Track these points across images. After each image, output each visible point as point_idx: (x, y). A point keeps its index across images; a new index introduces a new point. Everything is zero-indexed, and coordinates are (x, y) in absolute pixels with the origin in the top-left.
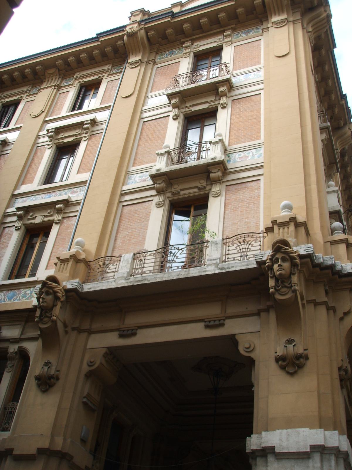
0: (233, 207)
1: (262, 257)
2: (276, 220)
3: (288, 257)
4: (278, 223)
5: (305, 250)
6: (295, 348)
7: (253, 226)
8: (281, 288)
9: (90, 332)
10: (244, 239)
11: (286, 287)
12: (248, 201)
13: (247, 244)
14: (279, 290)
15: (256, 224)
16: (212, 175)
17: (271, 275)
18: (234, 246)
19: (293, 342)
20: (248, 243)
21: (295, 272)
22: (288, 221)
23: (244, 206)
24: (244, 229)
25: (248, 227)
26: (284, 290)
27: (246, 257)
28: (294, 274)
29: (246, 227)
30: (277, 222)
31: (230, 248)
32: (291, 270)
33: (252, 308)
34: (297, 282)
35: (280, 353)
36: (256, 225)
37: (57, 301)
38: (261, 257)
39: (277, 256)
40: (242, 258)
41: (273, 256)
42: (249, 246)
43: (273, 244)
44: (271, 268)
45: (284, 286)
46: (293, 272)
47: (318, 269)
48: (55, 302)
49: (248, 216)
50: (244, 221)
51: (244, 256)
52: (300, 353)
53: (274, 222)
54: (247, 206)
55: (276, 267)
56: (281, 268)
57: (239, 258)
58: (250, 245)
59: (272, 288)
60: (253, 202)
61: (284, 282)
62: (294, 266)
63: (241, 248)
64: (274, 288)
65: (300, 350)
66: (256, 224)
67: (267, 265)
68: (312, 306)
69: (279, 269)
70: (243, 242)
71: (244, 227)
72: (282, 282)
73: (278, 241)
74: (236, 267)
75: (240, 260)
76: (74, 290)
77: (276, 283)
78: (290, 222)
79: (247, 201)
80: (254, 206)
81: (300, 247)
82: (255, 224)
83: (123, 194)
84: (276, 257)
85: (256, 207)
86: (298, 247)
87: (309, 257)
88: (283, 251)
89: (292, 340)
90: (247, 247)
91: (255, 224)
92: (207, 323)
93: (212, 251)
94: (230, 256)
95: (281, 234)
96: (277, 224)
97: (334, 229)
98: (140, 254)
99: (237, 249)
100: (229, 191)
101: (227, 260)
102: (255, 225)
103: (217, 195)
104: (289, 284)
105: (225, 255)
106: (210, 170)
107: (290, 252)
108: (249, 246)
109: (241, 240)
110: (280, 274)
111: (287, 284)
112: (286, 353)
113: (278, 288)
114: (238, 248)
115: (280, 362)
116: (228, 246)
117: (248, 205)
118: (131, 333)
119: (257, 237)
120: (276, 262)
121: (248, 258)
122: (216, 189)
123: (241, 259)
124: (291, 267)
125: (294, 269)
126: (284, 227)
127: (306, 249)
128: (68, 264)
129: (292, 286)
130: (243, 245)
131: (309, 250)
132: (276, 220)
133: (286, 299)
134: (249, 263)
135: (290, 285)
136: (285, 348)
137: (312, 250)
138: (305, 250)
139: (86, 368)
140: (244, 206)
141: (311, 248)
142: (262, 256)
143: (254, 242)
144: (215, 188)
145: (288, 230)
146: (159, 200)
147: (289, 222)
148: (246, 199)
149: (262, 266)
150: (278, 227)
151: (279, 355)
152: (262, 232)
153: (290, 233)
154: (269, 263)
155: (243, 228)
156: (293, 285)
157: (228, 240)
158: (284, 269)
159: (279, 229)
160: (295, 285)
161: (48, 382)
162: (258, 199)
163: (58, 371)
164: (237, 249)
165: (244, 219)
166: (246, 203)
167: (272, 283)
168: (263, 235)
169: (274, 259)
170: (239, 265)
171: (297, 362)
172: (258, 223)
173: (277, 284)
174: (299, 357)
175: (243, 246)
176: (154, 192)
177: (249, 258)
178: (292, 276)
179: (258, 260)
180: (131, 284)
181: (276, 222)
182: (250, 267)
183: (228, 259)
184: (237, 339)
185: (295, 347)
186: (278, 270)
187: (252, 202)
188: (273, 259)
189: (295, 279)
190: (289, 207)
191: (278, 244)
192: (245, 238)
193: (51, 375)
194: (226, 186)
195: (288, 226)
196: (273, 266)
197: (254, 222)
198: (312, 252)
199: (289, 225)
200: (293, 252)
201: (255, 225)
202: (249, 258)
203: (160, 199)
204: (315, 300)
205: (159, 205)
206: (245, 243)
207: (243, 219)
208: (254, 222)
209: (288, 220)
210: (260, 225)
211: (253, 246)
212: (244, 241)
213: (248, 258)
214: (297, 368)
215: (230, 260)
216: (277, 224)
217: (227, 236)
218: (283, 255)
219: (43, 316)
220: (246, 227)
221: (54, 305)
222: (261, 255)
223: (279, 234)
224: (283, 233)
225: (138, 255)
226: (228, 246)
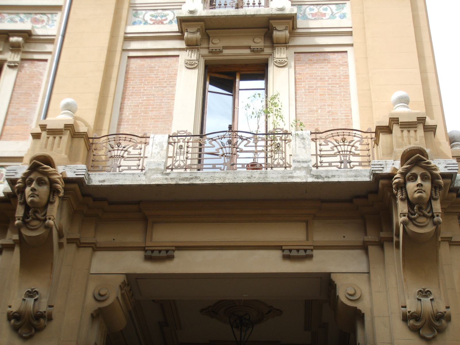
0: (309, 87)
1: (383, 168)
2: (398, 118)
3: (429, 175)
5: (446, 167)
6: (434, 304)
7: (342, 119)
8: (417, 217)
9: (96, 248)
10: (342, 137)
11: (424, 216)
12: (330, 80)
13: (348, 145)
14: (415, 219)
15: (346, 116)
16: (276, 34)
17: (402, 196)
18: (328, 145)
19: (428, 294)
20: (350, 144)
21: (437, 197)
22: (416, 122)
23: (324, 87)
24: (328, 121)
25: (333, 119)
27: (348, 164)
28: (435, 199)
29: (331, 118)
31: (324, 148)
32: (431, 194)
33: (353, 236)
36: (346, 118)
37: (53, 195)
38: (382, 169)
39: (414, 171)
40: (343, 164)
41: (408, 170)
42: (351, 149)
43: (405, 151)
44: (402, 186)
45: (422, 214)
46: (435, 197)
47: (454, 195)
48: (51, 197)
49: (332, 103)
50: (327, 110)
51: (345, 162)
53: (394, 120)
54: (330, 88)
55: (411, 186)
57: (339, 164)
58: (354, 148)
59: (404, 216)
60: (339, 84)
62: (435, 188)
63: (340, 150)
64: (407, 215)
66: (346, 116)
67: (396, 181)
68: (447, 244)
69: (418, 190)
70: (342, 141)
71: (327, 117)
72: (420, 209)
73: (412, 150)
74: (339, 176)
75: (340, 168)
76: (79, 182)
77: (411, 211)
78: (418, 123)
79: (329, 81)
80: (340, 89)
81: (438, 162)
82: (345, 116)
83: (127, 39)
84: (411, 173)
85: (344, 92)
86: (435, 162)
88: (424, 165)
89: (428, 291)
90: (349, 150)
91: (345, 116)
92: (287, 253)
93: (297, 148)
94: (324, 159)
95: (406, 139)
97: (453, 139)
98: (179, 138)
99: (333, 150)
100: (299, 62)
101: (319, 164)
102: (344, 117)
103: (282, 65)
105: (316, 155)
106: (272, 26)
107: (433, 168)
108: (351, 149)
109: (339, 138)
111: (426, 213)
112: (420, 309)
113: (413, 217)
114: (335, 148)
116: (320, 145)
117: (332, 87)
118: (167, 255)
119: (362, 137)
120: (412, 179)
121: (352, 166)
122: (280, 54)
123: (341, 166)
124: (432, 190)
125: (435, 191)
126: (409, 129)
127: (447, 165)
128: (61, 138)
129: (433, 217)
130: (343, 146)
131: (453, 168)
132: (398, 118)
133: (424, 233)
134: (358, 173)
135: (430, 214)
136: (419, 302)
137: (457, 168)
138: (446, 167)
139: (92, 305)
140: (324, 87)
141: (455, 165)
142: (382, 166)
143: (359, 143)
144: (279, 54)
145: (416, 135)
146: (191, 57)
147: (417, 123)
148: (327, 78)
149: (382, 182)
150: (400, 128)
151: (411, 311)
152: (369, 131)
153: (418, 139)
154: (400, 179)
155: (326, 119)
156: (435, 214)
157: (318, 135)
158: (424, 191)
159: (402, 131)
160: (438, 216)
161: (35, 323)
162: (346, 80)
163: (50, 306)
164: (333, 150)
165: (327, 107)
166: (328, 84)
167: (402, 207)
168: (371, 135)
169: (409, 174)
170: (343, 174)
171: (437, 324)
172: (348, 116)
175: (342, 147)
176: (181, 44)
177: (354, 166)
179: (377, 172)
180: (174, 182)
182: (359, 179)
183: (321, 162)
184: (333, 280)
185: (432, 302)
186: (416, 191)
187: (337, 84)
188: (408, 176)
189: (437, 206)
190: (404, 101)
191: (418, 155)
192: (345, 137)
193: (40, 312)
194: (295, 53)
195: (415, 129)
196: (405, 183)
197: (342, 114)
198: (456, 171)
199: (416, 127)
200: (436, 168)
201: (344, 117)
202: (353, 165)
203: (193, 56)
204: (451, 238)
205: (190, 66)
206: (345, 143)
207: (325, 105)
208: (342, 114)
209: (416, 121)
210: (352, 118)
211: (357, 149)
212: (344, 140)
213: (352, 166)
214: (436, 332)
215: (324, 164)
216: (399, 123)
217: (317, 129)
218: (422, 171)
219: (30, 218)
220: (331, 118)
221: (49, 202)
222: (381, 165)
224: (409, 137)
225: (175, 138)
226: (320, 145)
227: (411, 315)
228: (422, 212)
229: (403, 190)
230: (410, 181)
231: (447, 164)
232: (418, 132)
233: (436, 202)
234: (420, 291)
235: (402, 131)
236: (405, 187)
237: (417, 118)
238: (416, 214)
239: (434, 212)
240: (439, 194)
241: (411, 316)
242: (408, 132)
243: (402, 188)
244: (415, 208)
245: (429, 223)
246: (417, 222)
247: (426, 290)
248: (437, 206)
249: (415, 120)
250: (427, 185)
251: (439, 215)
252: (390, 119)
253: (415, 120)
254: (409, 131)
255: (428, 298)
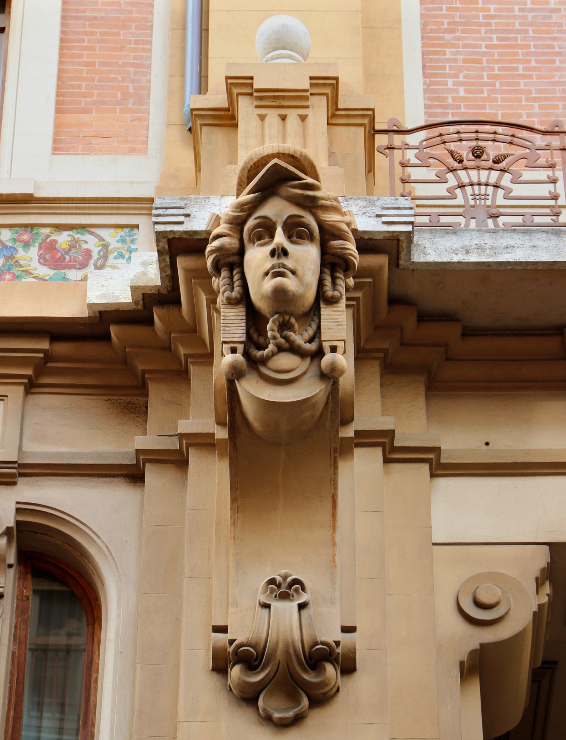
4: (258, 91)
8: (273, 354)
21: (336, 293)
22: (306, 91)
26: (286, 361)
28: (332, 301)
30: (256, 86)
34: (345, 338)
35: (240, 633)
52: (324, 639)
55: (257, 258)
56: (284, 266)
61: (290, 327)
65: (330, 634)
69: (273, 267)
87: (391, 246)
89: (296, 581)
96: (255, 94)
104: (310, 341)
110: (280, 293)
113: (259, 354)
115: (236, 672)
124: (322, 272)
129: (319, 353)
135: (313, 347)
138: (378, 216)
158: (294, 273)
159: (262, 118)
160: (334, 349)
173: (255, 336)
174: (319, 656)
178: (322, 310)
181: (252, 85)
185: (304, 612)
186: (267, 274)
195: (303, 112)
196: (241, 252)
199: (307, 107)
204: (391, 434)
209: (307, 86)
216: (255, 94)
223: (260, 137)
227: (236, 652)
228: (287, 339)
229: (235, 272)
230: (254, 243)
231: (384, 208)
232: (311, 119)
233: (335, 309)
234: (272, 581)
235: (262, 118)
236: (241, 264)
237: (311, 78)
238: (271, 347)
239: (323, 338)
240: (346, 282)
241: (236, 654)
242: (280, 120)
243: (231, 268)
244: (269, 326)
245: (304, 373)
246: (270, 369)
247: (289, 579)
248: (337, 324)
249: (305, 84)
250: (306, 257)
251: (338, 349)
252: (229, 81)
253: (305, 84)
254: (283, 118)
255: (292, 601)
